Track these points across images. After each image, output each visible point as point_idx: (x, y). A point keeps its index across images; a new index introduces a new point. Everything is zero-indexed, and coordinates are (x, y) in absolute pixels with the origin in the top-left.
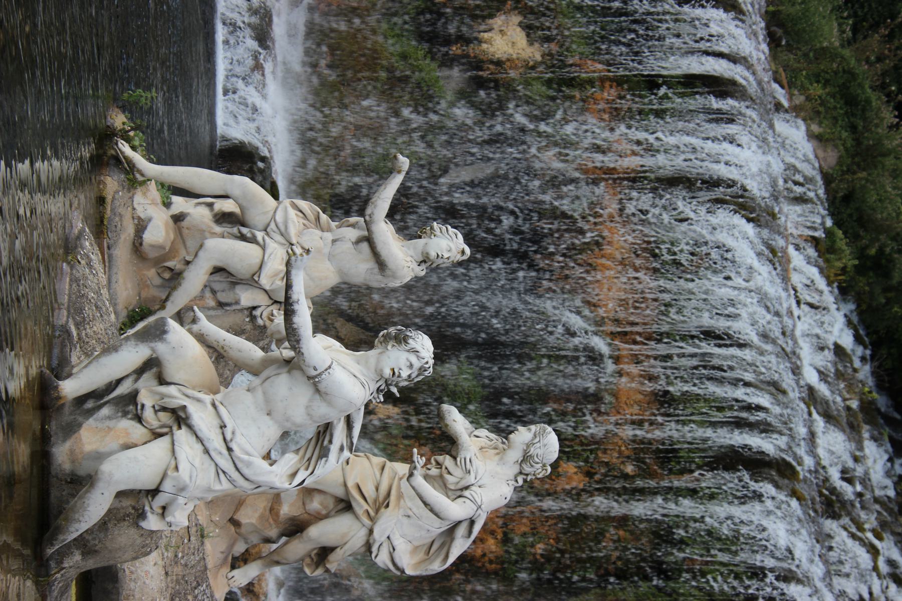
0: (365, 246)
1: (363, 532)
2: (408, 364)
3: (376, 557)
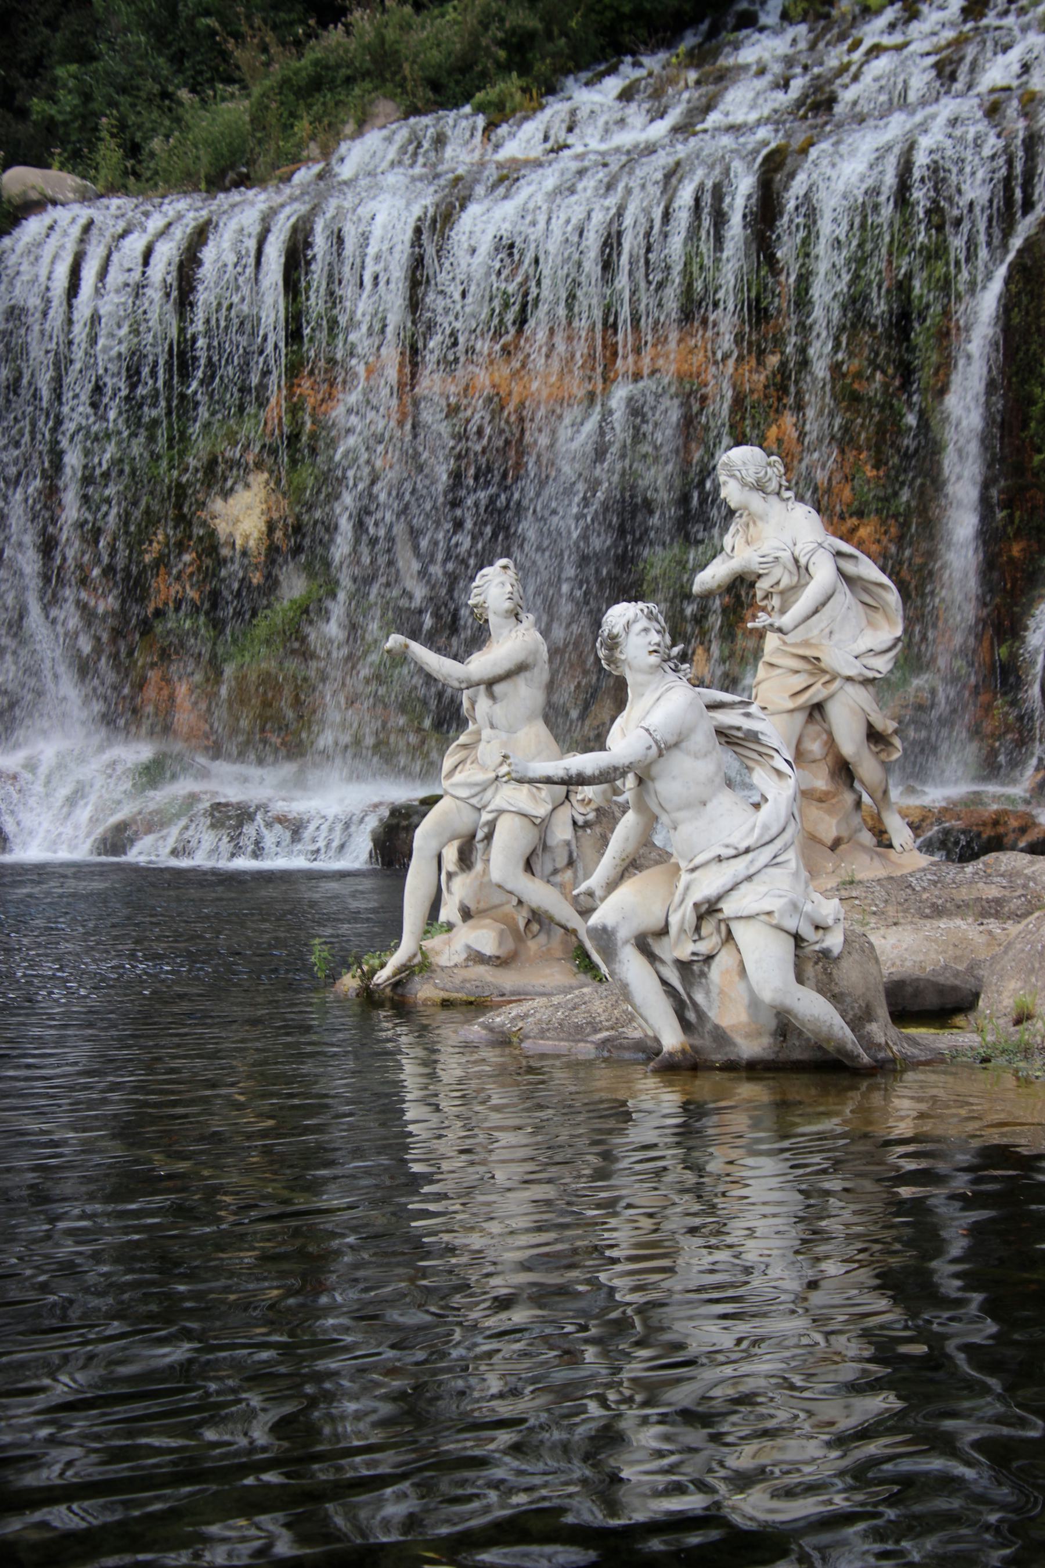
0: (498, 689)
1: (851, 689)
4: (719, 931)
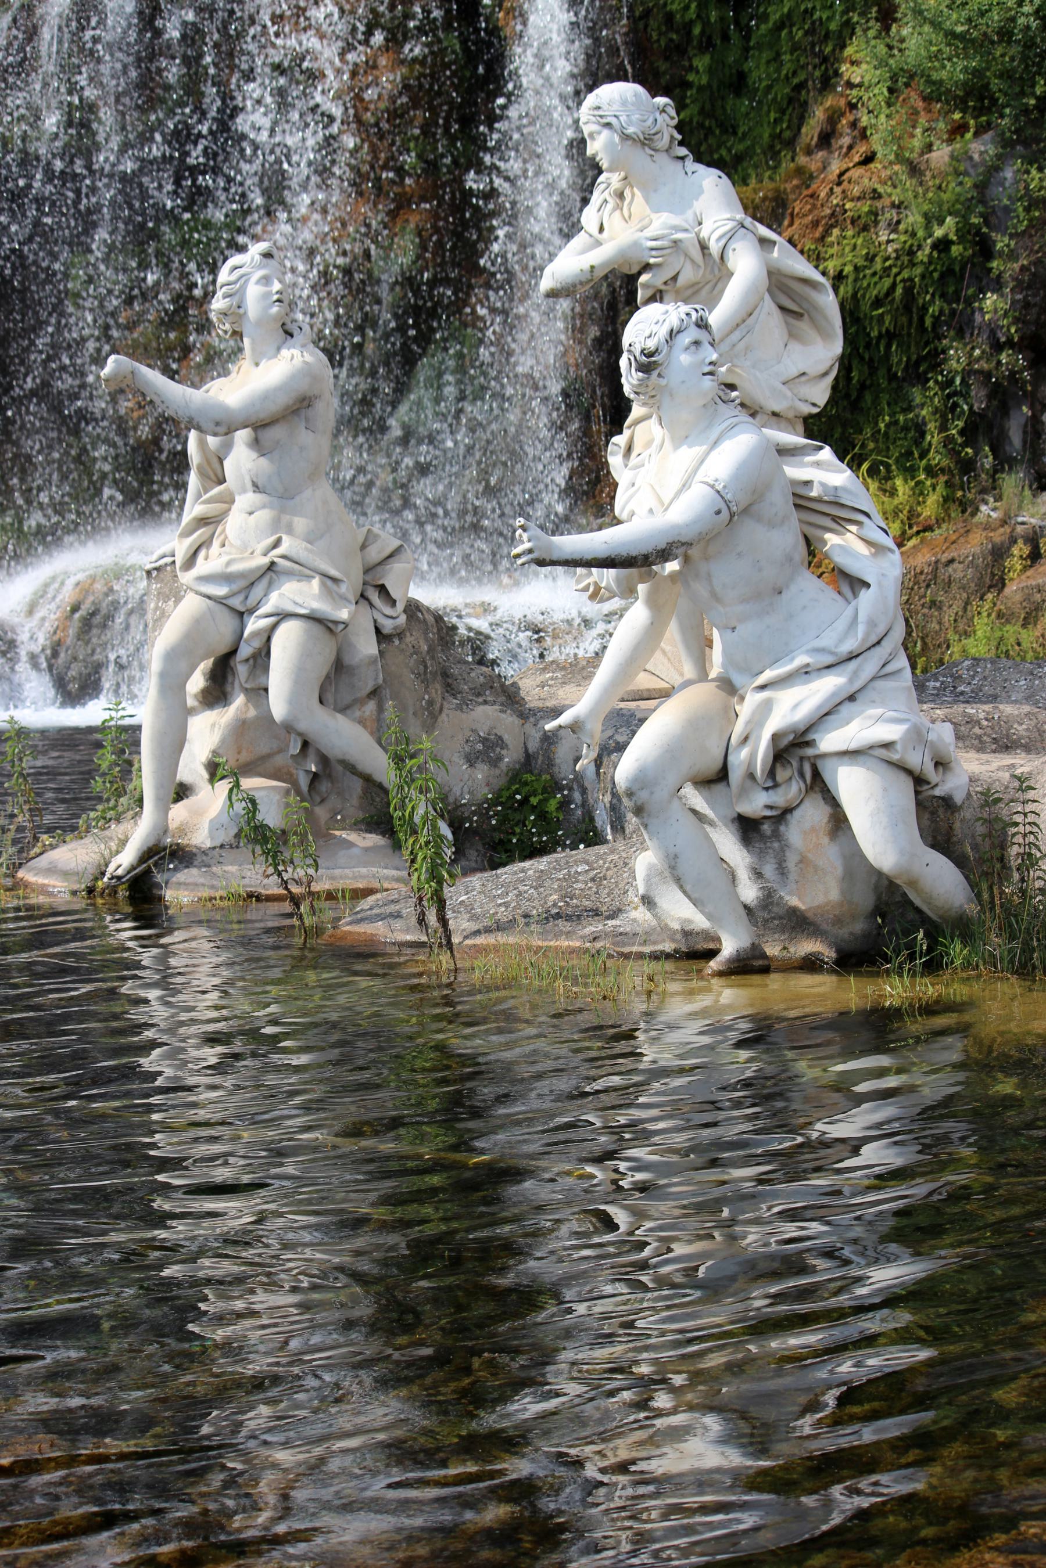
2: (693, 348)
3: (814, 405)
4: (802, 775)
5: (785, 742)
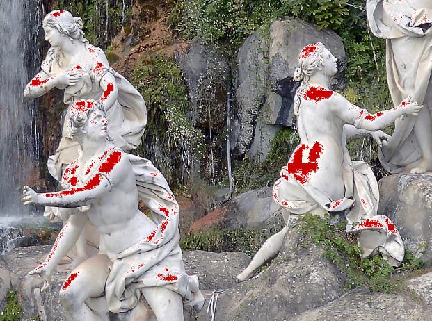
5: (130, 281)
